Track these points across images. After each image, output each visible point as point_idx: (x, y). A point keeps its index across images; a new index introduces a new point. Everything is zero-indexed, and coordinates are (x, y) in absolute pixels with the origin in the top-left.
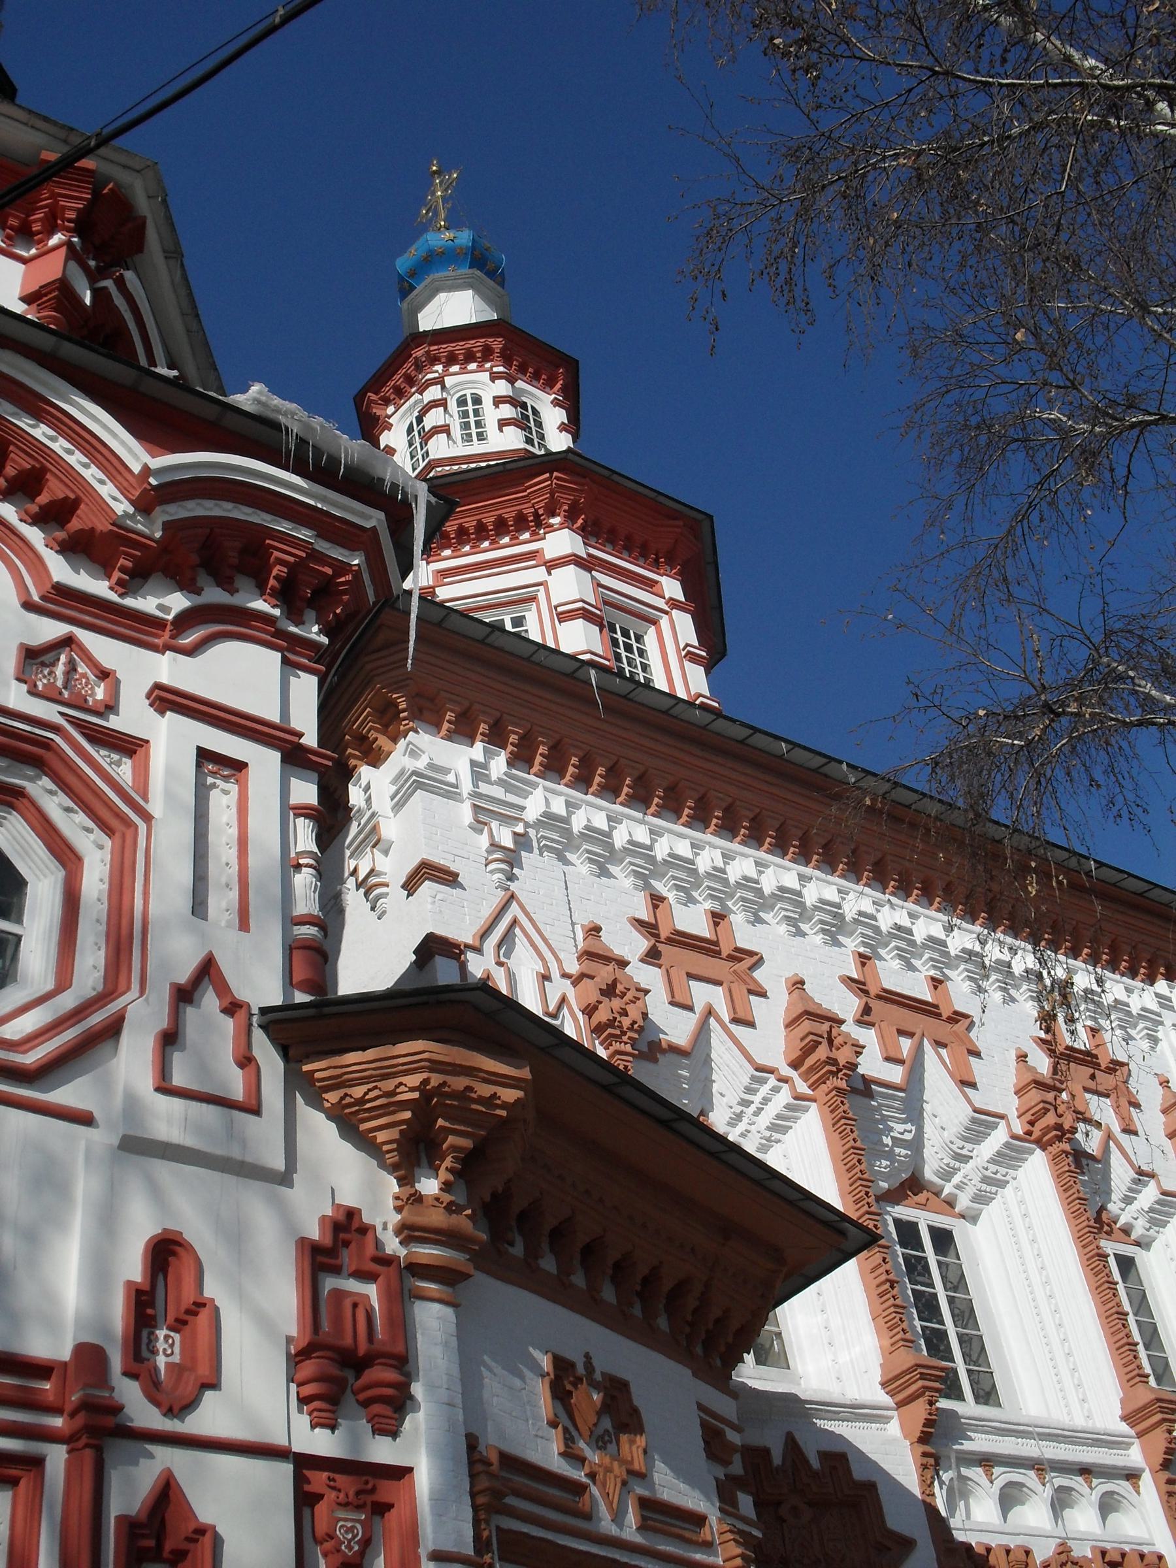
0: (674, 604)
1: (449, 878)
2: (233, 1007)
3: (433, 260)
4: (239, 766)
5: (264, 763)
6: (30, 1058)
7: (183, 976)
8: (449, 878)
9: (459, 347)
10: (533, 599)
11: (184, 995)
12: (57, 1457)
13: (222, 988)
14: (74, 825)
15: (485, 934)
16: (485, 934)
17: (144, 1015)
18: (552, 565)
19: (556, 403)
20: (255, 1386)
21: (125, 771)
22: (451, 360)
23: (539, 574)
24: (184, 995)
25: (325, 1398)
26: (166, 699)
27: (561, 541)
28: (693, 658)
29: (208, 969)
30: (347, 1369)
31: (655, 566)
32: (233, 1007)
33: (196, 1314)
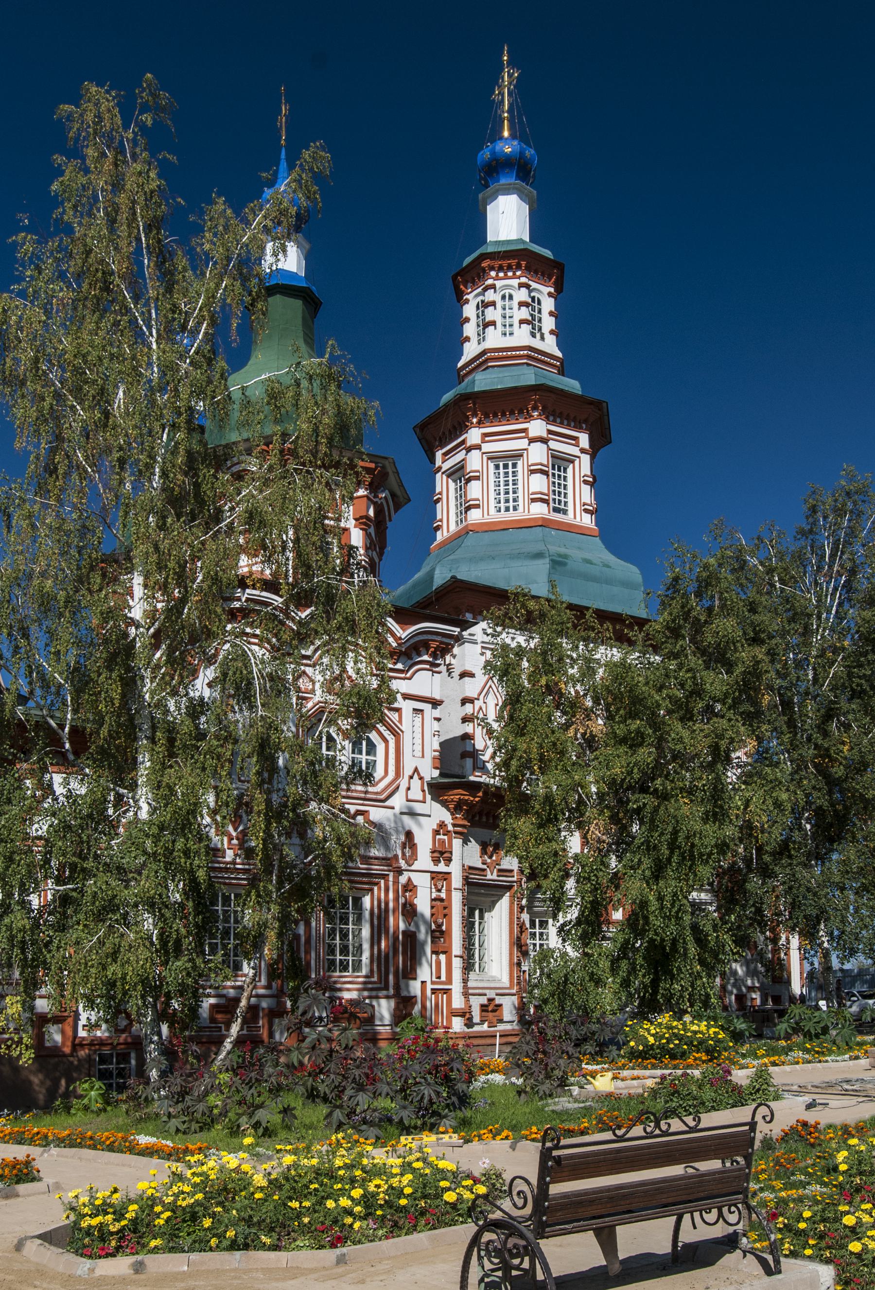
0: (583, 451)
1: (472, 675)
2: (421, 778)
3: (496, 167)
4: (422, 711)
5: (427, 707)
6: (382, 797)
7: (410, 773)
8: (472, 675)
9: (505, 263)
10: (522, 456)
11: (411, 777)
12: (391, 874)
13: (419, 774)
14: (386, 733)
15: (480, 694)
16: (480, 694)
17: (404, 783)
18: (532, 441)
19: (550, 295)
20: (424, 860)
21: (396, 715)
22: (501, 269)
23: (523, 444)
24: (411, 777)
25: (436, 861)
26: (406, 697)
27: (537, 427)
28: (586, 482)
29: (416, 770)
30: (441, 854)
31: (578, 427)
32: (421, 778)
33: (413, 846)
